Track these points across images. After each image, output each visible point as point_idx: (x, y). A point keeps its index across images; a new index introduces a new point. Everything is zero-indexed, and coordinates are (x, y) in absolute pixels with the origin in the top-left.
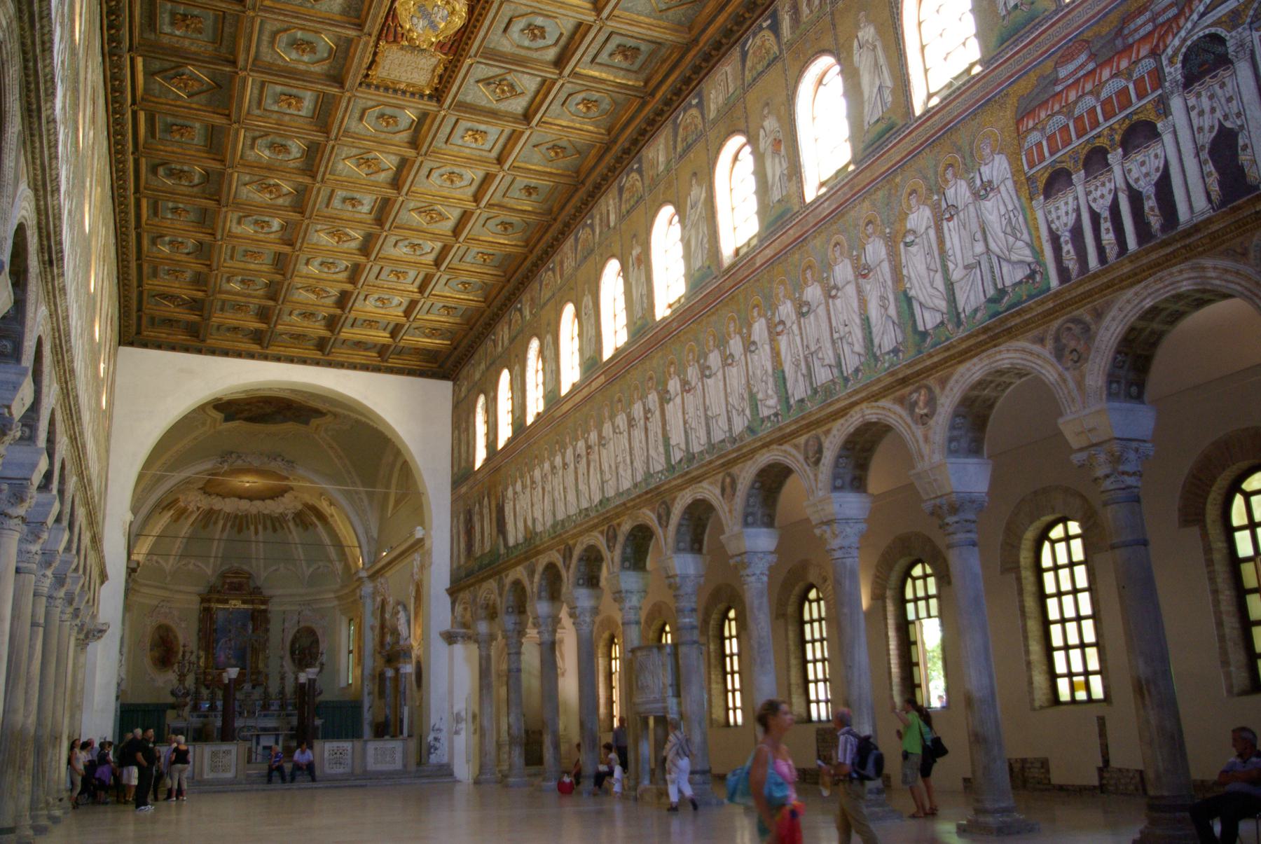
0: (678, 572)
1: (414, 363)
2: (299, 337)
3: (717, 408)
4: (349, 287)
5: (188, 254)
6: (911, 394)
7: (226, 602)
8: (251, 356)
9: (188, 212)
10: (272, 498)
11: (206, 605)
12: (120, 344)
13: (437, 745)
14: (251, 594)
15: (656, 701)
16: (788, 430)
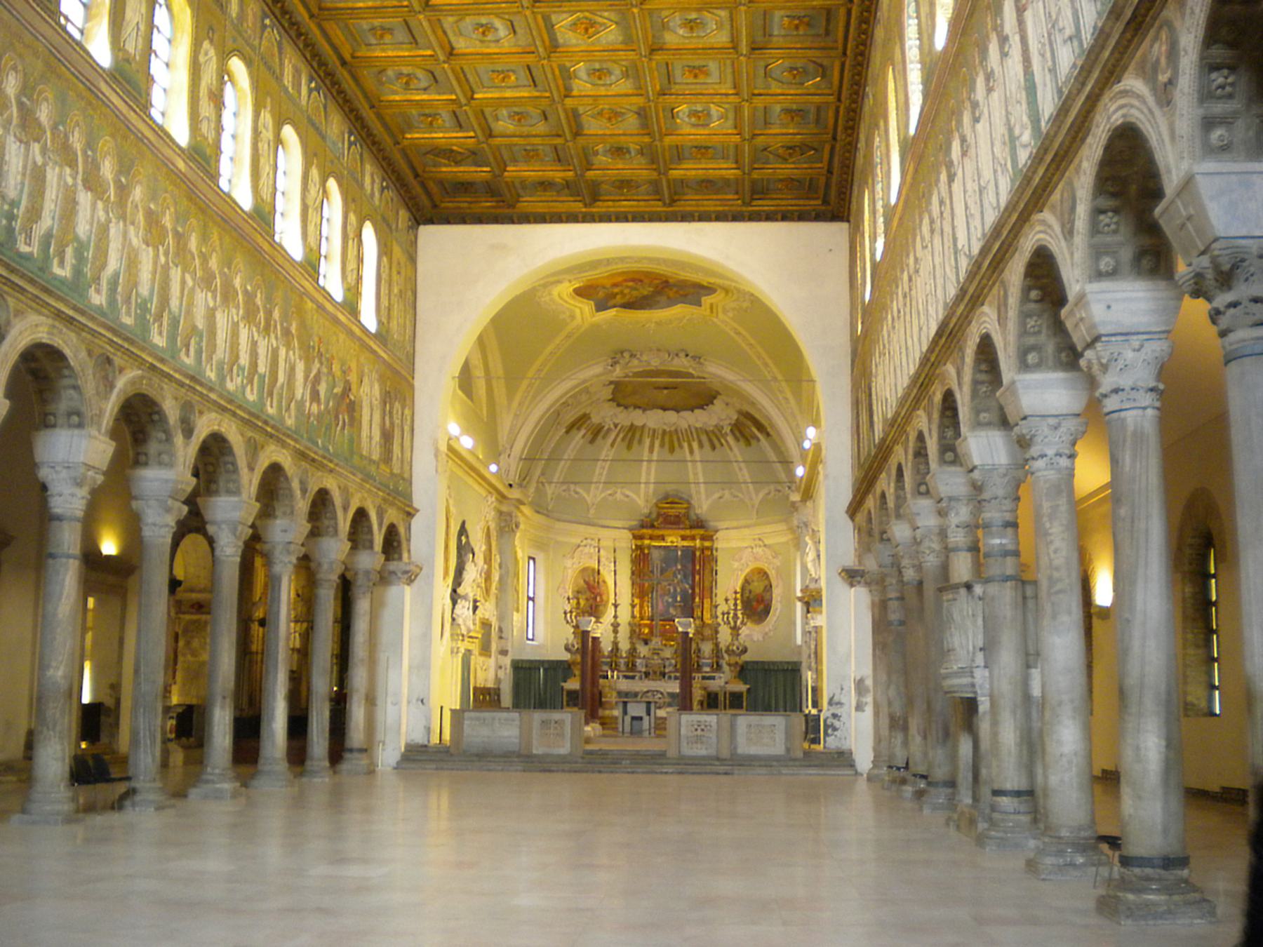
0: (977, 461)
1: (788, 204)
2: (624, 185)
3: (987, 174)
4: (640, 101)
5: (425, 89)
6: (1151, 47)
7: (663, 538)
8: (572, 218)
9: (390, 31)
10: (701, 407)
11: (639, 543)
12: (419, 224)
13: (837, 723)
14: (691, 528)
15: (962, 672)
16: (1037, 179)
